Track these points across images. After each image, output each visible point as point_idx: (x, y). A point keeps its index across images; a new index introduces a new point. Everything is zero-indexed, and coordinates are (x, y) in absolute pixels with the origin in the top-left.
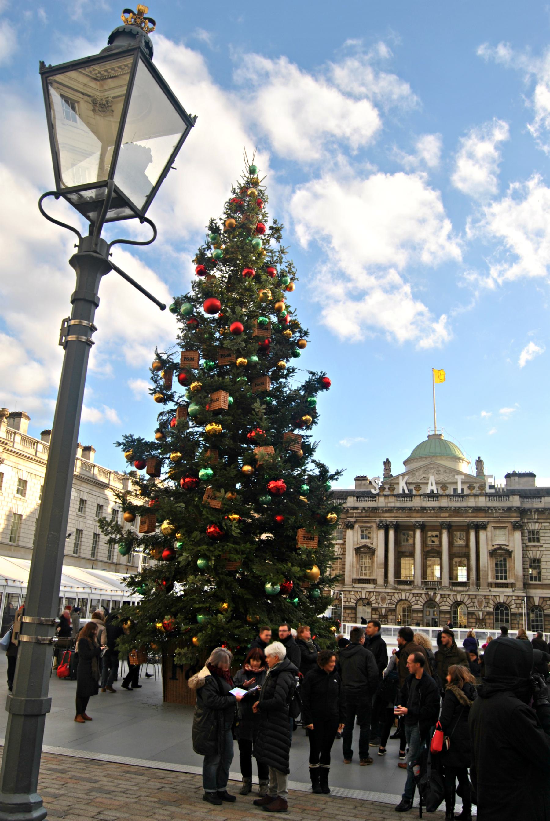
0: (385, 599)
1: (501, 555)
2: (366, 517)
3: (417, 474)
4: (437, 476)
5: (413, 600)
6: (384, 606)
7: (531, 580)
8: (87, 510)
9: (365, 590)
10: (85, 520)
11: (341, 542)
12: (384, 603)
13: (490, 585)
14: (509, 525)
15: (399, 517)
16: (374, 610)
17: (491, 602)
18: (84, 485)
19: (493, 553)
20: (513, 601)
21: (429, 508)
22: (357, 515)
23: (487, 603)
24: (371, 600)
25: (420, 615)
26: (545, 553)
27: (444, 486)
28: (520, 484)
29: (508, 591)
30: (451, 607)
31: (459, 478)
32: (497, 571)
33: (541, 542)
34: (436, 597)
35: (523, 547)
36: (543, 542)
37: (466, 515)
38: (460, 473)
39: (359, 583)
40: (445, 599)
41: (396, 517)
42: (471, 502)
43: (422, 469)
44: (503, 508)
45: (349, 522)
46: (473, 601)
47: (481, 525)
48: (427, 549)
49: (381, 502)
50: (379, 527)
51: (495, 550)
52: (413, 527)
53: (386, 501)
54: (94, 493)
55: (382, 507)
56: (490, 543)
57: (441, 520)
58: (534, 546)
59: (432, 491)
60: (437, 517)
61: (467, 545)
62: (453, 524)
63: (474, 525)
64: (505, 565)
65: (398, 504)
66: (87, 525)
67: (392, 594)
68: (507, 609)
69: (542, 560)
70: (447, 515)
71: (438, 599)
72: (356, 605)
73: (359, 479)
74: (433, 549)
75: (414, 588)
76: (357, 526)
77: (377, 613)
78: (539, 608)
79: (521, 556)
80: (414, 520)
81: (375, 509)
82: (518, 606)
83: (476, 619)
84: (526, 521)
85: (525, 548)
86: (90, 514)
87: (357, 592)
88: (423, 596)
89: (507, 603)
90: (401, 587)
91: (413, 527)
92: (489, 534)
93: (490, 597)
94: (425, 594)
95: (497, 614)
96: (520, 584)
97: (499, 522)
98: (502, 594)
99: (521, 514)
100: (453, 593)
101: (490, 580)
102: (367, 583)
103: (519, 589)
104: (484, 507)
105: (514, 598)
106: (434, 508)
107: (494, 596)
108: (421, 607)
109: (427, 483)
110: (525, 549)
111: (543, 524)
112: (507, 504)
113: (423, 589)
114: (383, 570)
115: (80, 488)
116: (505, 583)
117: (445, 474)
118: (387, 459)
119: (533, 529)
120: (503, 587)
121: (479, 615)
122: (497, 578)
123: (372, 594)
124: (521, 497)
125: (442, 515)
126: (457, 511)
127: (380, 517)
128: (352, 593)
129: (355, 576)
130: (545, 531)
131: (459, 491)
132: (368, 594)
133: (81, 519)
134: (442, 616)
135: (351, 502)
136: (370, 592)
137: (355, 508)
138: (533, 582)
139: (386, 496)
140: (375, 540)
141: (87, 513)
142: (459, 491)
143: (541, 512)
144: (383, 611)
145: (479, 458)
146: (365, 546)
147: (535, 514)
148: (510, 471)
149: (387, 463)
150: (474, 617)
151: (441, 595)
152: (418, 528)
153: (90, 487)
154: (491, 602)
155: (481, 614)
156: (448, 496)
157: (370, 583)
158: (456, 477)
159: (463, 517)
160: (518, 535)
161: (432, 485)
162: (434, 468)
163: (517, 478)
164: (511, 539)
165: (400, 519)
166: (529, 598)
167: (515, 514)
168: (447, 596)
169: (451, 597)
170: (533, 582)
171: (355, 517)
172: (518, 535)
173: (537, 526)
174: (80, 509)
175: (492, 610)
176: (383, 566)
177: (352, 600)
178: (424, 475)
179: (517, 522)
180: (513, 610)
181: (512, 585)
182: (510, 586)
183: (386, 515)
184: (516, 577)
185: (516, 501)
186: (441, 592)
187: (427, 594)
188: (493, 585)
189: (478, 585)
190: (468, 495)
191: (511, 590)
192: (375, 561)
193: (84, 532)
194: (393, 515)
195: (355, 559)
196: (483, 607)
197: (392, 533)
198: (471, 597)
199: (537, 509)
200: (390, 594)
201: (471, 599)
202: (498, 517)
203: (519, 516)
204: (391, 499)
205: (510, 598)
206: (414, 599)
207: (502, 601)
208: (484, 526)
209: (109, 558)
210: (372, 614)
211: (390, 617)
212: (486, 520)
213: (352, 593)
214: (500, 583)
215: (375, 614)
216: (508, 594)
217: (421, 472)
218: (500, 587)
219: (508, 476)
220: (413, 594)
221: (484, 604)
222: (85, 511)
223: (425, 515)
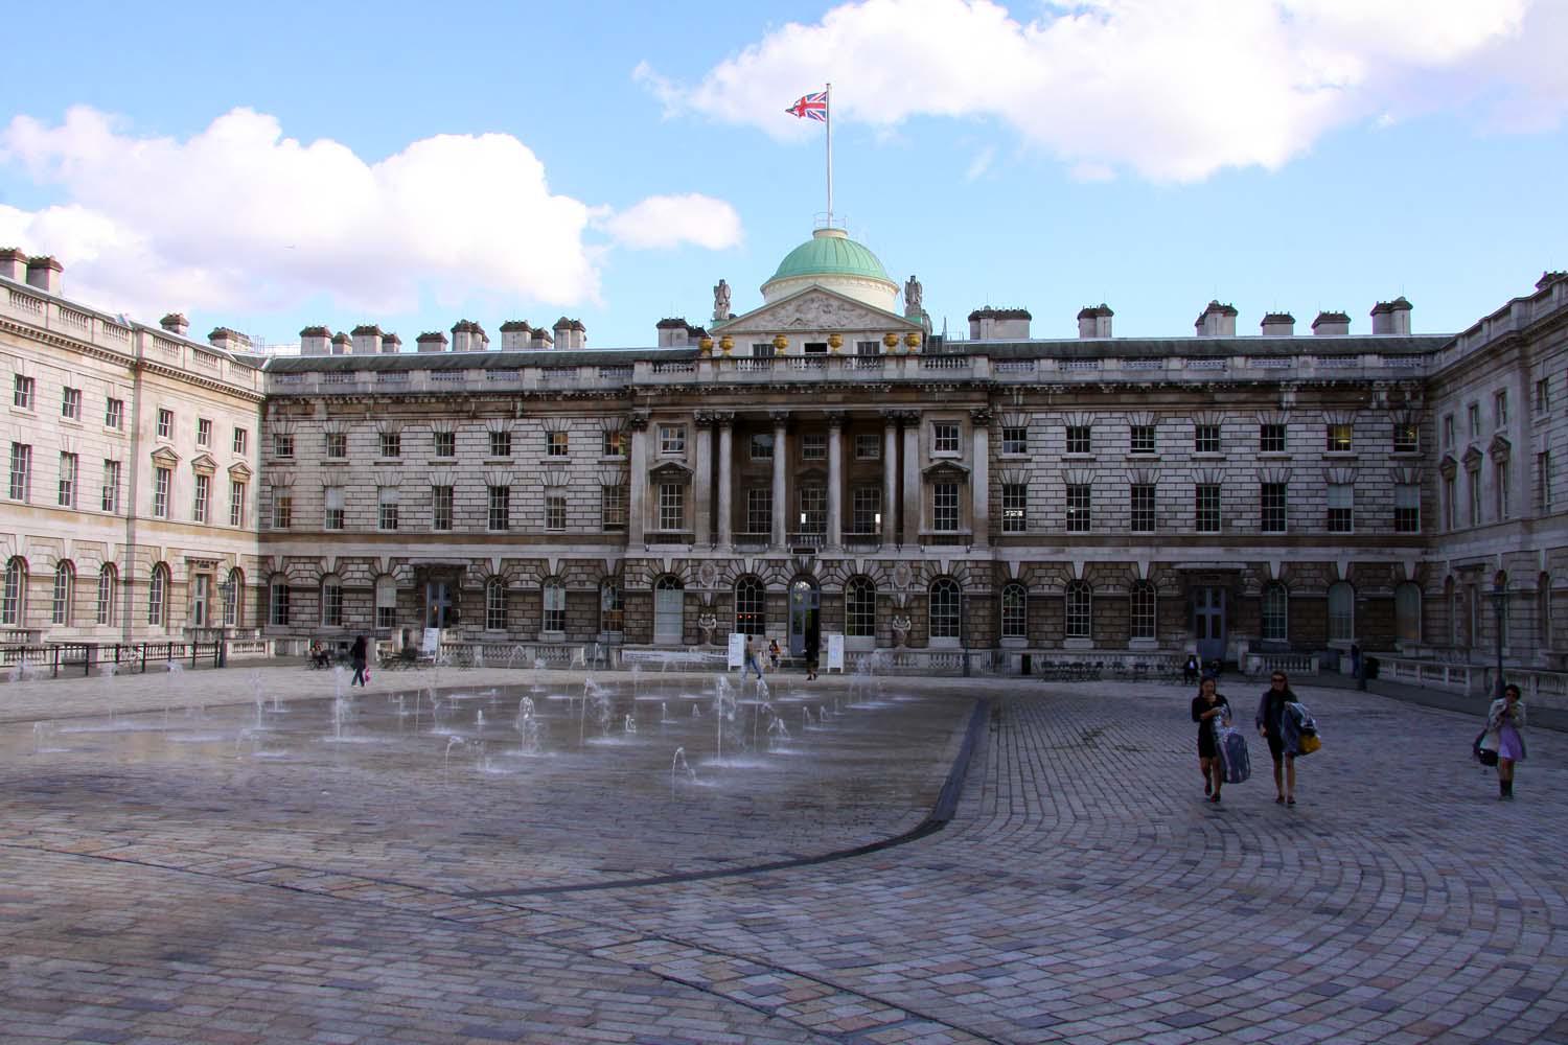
0: (712, 573)
1: (947, 481)
2: (673, 404)
3: (783, 312)
5: (765, 573)
6: (709, 588)
7: (1006, 529)
8: (37, 399)
9: (669, 555)
10: (34, 424)
11: (621, 457)
12: (710, 581)
13: (923, 540)
14: (963, 417)
15: (740, 404)
16: (690, 596)
17: (924, 574)
18: (23, 343)
19: (929, 476)
20: (967, 571)
21: (803, 382)
22: (655, 401)
23: (916, 576)
24: (683, 575)
25: (782, 603)
26: (1035, 473)
28: (997, 335)
29: (957, 552)
30: (734, 586)
32: (938, 512)
33: (1029, 451)
34: (814, 568)
36: (1034, 451)
37: (879, 399)
39: (658, 543)
40: (832, 570)
41: (734, 404)
42: (891, 372)
43: (794, 304)
44: (953, 383)
45: (637, 415)
47: (906, 418)
48: (800, 470)
49: (705, 373)
50: (699, 425)
51: (934, 470)
52: (767, 425)
53: (716, 370)
54: (50, 361)
55: (704, 383)
56: (924, 455)
57: (826, 409)
58: (1015, 461)
60: (819, 403)
61: (881, 462)
63: (895, 418)
64: (954, 501)
65: (739, 378)
67: (726, 564)
68: (954, 588)
69: (1029, 487)
70: (839, 397)
71: (817, 570)
72: (542, 587)
73: (664, 325)
74: (814, 470)
75: (772, 548)
76: (653, 424)
78: (1018, 586)
79: (986, 481)
80: (771, 409)
81: (692, 389)
82: (977, 580)
83: (894, 608)
84: (999, 408)
85: (995, 464)
87: (654, 560)
88: (789, 564)
89: (956, 574)
90: (745, 547)
91: (767, 425)
92: (924, 436)
94: (793, 561)
95: (935, 599)
96: (981, 537)
97: (945, 411)
98: (946, 557)
99: (990, 394)
100: (848, 557)
101: (923, 531)
102: (676, 542)
103: (980, 548)
104: (916, 381)
105: (968, 565)
106: (812, 385)
108: (784, 588)
110: (996, 466)
111: (1035, 416)
112: (963, 375)
113: (789, 551)
114: (708, 514)
115: (9, 350)
116: (953, 536)
118: (722, 281)
119: (1014, 424)
120: (948, 544)
121: (899, 601)
122: (938, 527)
123: (684, 564)
124: (989, 360)
125: (830, 397)
126: (857, 391)
127: (703, 404)
128: (645, 563)
129: (650, 530)
130: (1036, 430)
132: (676, 564)
133: (21, 421)
134: (827, 604)
135: (642, 374)
136: (680, 560)
137: (647, 387)
138: (1011, 533)
139: (715, 361)
140: (691, 452)
143: (1029, 390)
144: (708, 597)
145: (913, 277)
146: (671, 466)
147: (1018, 395)
148: (980, 307)
149: (721, 290)
150: (889, 604)
151: (824, 561)
152: (779, 426)
153: (38, 347)
154: (924, 574)
155: (903, 598)
156: (842, 358)
157: (680, 542)
159: (871, 402)
160: (981, 440)
163: (991, 321)
164: (967, 446)
165: (742, 409)
166: (998, 566)
167: (976, 396)
168: (836, 564)
169: (845, 567)
170: (1011, 533)
171: (650, 405)
172: (981, 440)
173: (1021, 420)
175: (925, 589)
176: (707, 506)
177: (645, 578)
178: (798, 315)
179: (980, 412)
180: (966, 590)
181: (968, 540)
182: (962, 541)
183: (714, 399)
184: (973, 524)
185: (982, 369)
186: (825, 556)
187: (795, 561)
188: (930, 540)
189: (899, 541)
191: (963, 548)
192: (692, 496)
194: (728, 399)
195: (650, 495)
196: (906, 585)
197: (726, 440)
198: (884, 564)
199: (1023, 384)
200: (721, 563)
201: (885, 568)
202: (942, 402)
203: (986, 397)
204: (724, 367)
205: (962, 565)
206: (770, 571)
207: (945, 572)
208: (913, 421)
209: (106, 505)
210: (685, 604)
211: (721, 609)
212: (918, 407)
213: (645, 563)
214: (943, 536)
215: (691, 604)
216: (958, 558)
217: (791, 308)
218: (943, 544)
219: (975, 317)
221: (910, 579)
223: (795, 398)
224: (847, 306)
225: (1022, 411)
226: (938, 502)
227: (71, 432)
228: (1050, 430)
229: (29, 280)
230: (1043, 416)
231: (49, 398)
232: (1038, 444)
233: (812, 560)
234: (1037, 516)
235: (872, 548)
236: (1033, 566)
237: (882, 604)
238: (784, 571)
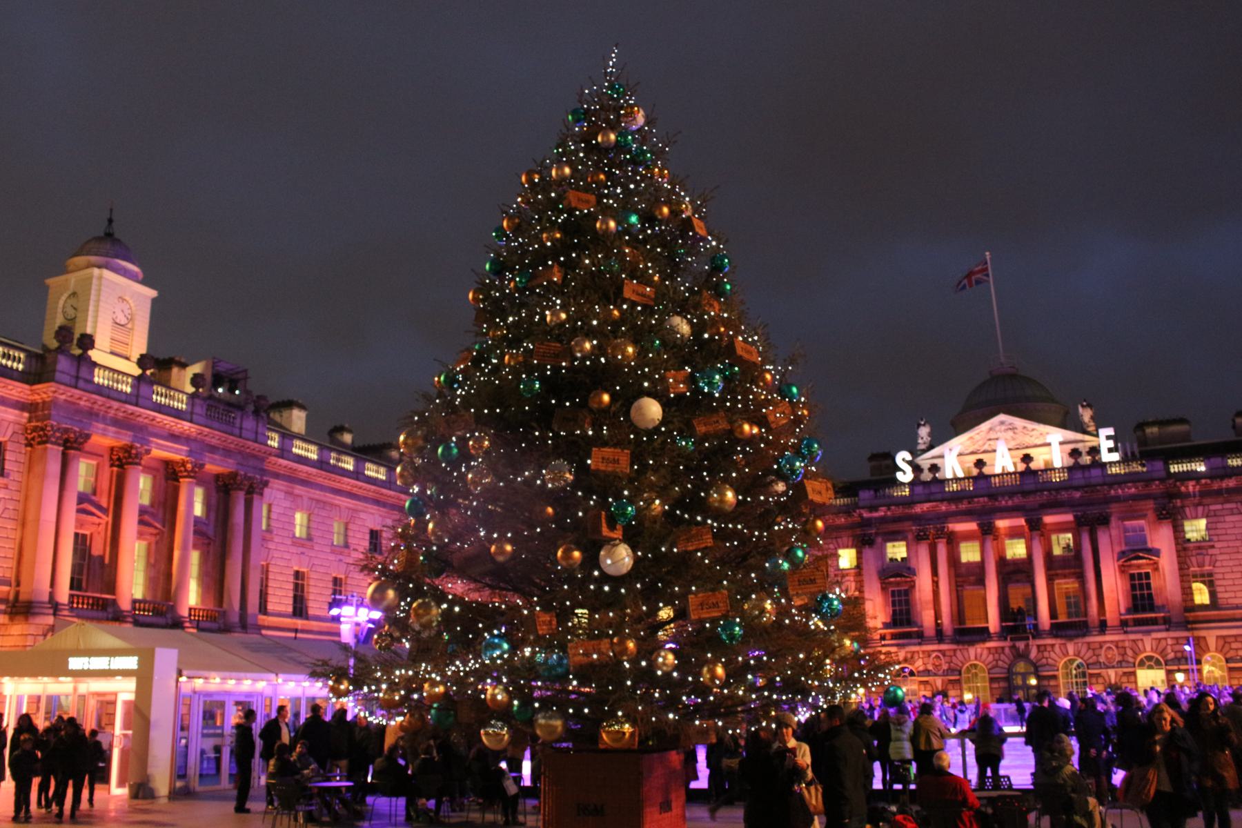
35: (1178, 551)
40: (1046, 654)
46: (1097, 652)
71: (1033, 653)
77: (929, 687)
93: (1127, 644)
107: (1134, 641)
110: (1182, 554)
111: (1212, 507)
150: (1101, 680)
151: (1038, 646)
168: (1049, 648)
176: (931, 606)
205: (1163, 642)
220: (989, 649)
225: (1200, 504)
226: (1133, 587)
228: (1228, 518)
230: (1219, 507)
232: (1219, 532)
233: (1027, 646)
234: (1226, 595)
236: (1229, 640)
237: (1094, 680)
238: (1003, 657)
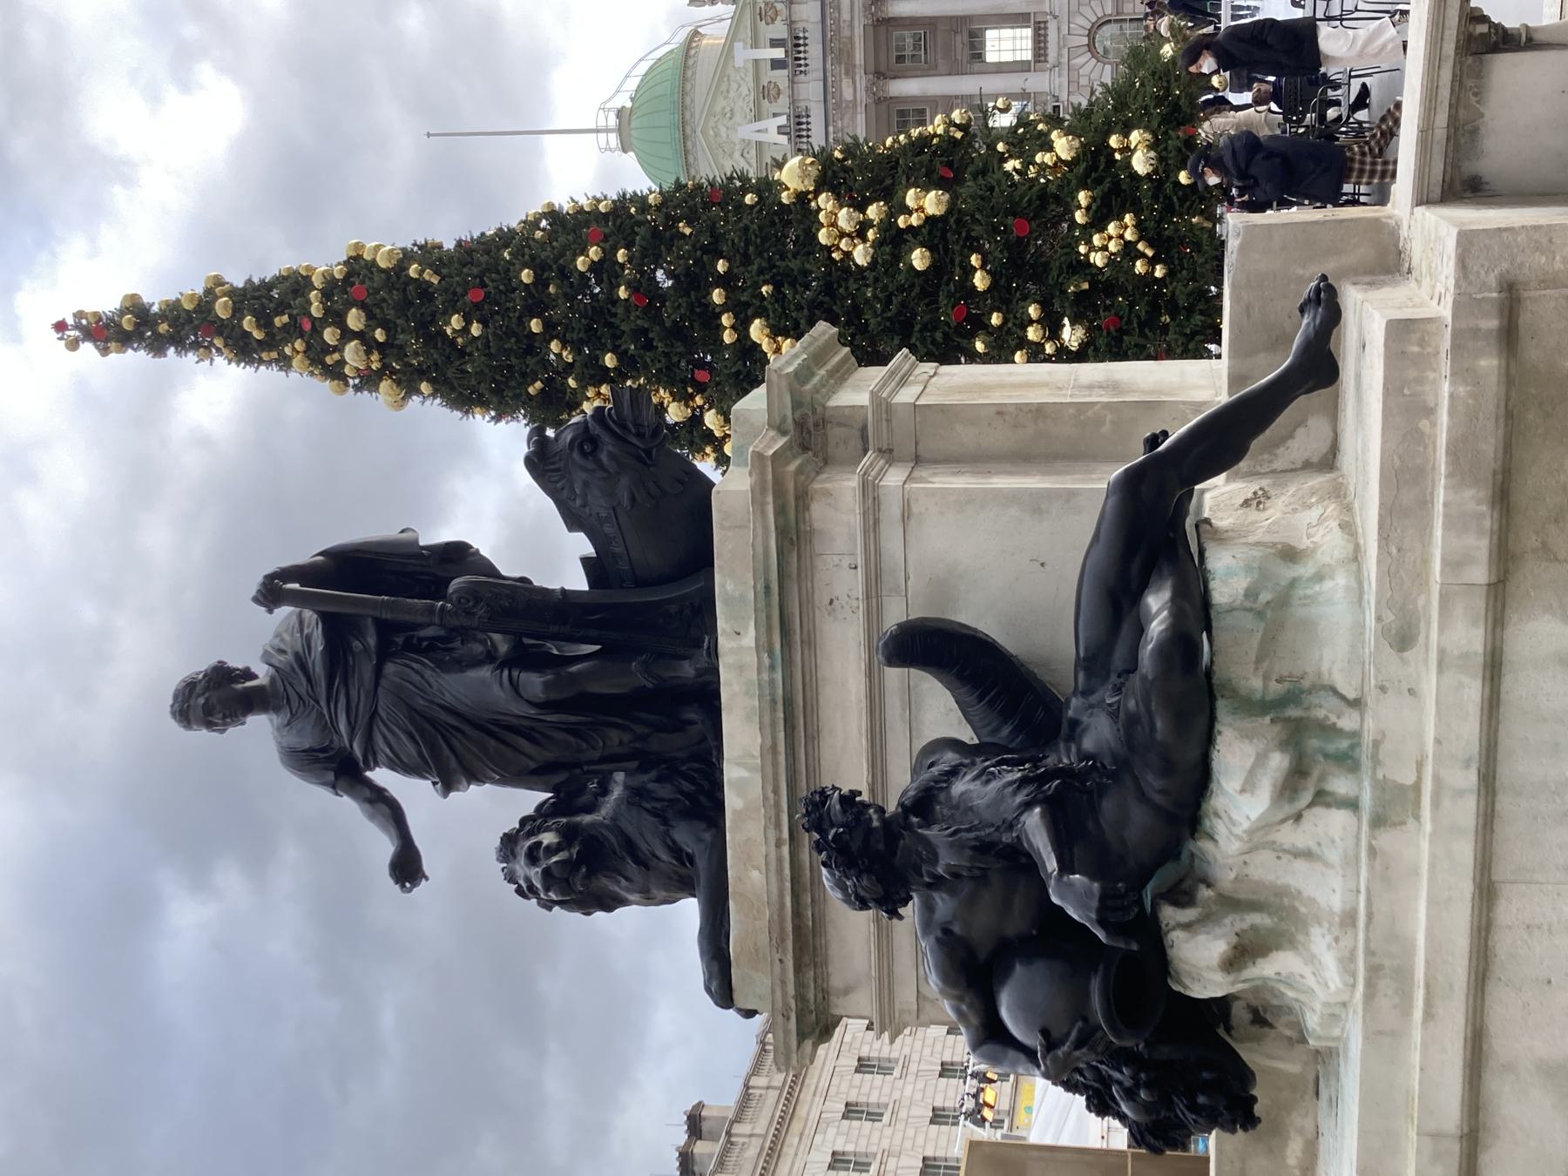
4: (738, 117)
8: (873, 1099)
10: (905, 1102)
18: (802, 1111)
27: (766, 93)
31: (744, 54)
38: (728, 51)
40: (1084, 81)
54: (824, 1084)
59: (781, 130)
62: (872, 68)
66: (918, 1096)
86: (886, 1090)
109: (759, 144)
115: (812, 1124)
117: (732, 94)
131: (779, 53)
141: (884, 1100)
142: (779, 53)
153: (806, 1096)
158: (739, 63)
161: (766, 131)
162: (715, 128)
174: (874, 1117)
178: (737, 155)
190: (791, 24)
193: (929, 1153)
222: (878, 1105)
224: (724, 87)
227: (913, 1068)
229: (714, 1138)
231: (871, 1089)
235: (1052, 27)
